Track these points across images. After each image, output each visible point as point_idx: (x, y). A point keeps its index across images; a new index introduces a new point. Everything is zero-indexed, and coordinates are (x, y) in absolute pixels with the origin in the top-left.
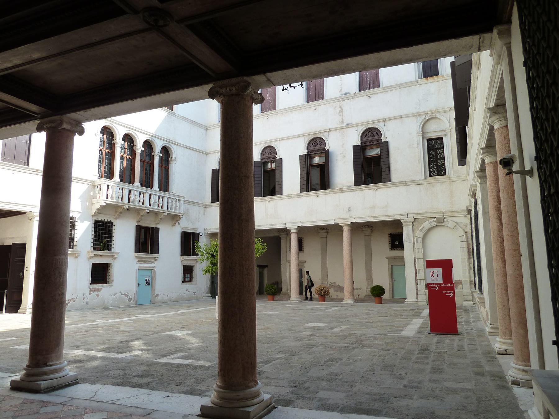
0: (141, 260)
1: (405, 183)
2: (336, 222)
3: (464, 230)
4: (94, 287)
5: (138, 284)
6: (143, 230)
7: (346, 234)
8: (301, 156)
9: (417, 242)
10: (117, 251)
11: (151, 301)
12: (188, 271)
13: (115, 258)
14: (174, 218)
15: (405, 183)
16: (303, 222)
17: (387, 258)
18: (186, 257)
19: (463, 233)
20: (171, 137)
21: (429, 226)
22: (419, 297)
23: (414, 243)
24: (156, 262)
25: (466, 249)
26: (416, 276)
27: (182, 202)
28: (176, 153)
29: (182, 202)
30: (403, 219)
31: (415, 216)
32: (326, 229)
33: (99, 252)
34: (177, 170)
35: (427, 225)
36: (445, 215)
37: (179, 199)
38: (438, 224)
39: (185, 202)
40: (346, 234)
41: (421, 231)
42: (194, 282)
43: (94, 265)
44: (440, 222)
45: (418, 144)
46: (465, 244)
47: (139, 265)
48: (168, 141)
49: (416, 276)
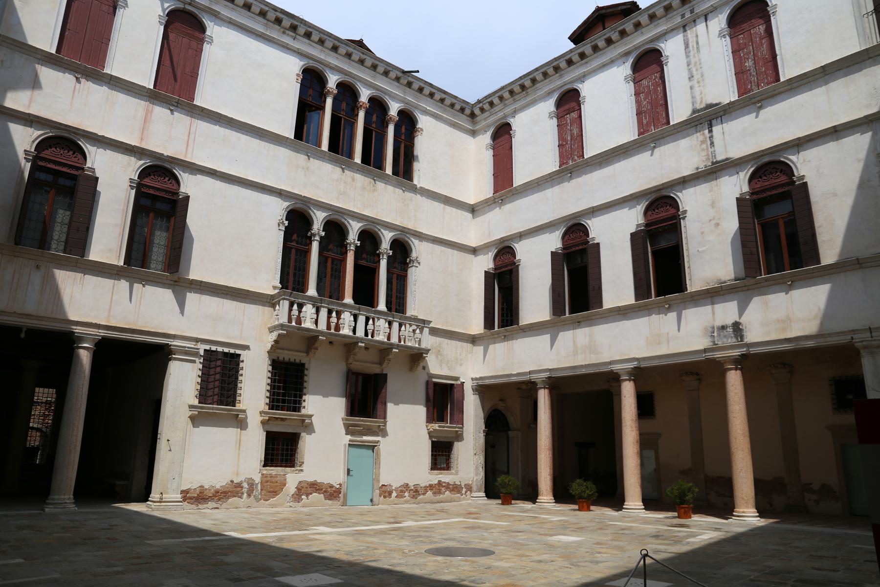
2: (709, 355)
4: (271, 472)
5: (349, 471)
6: (360, 378)
8: (632, 234)
10: (310, 413)
11: (371, 500)
14: (416, 357)
16: (644, 359)
18: (436, 426)
20: (410, 225)
27: (426, 330)
28: (419, 249)
29: (426, 330)
32: (697, 374)
33: (279, 413)
34: (419, 279)
37: (422, 323)
39: (435, 332)
47: (349, 437)
48: (404, 230)
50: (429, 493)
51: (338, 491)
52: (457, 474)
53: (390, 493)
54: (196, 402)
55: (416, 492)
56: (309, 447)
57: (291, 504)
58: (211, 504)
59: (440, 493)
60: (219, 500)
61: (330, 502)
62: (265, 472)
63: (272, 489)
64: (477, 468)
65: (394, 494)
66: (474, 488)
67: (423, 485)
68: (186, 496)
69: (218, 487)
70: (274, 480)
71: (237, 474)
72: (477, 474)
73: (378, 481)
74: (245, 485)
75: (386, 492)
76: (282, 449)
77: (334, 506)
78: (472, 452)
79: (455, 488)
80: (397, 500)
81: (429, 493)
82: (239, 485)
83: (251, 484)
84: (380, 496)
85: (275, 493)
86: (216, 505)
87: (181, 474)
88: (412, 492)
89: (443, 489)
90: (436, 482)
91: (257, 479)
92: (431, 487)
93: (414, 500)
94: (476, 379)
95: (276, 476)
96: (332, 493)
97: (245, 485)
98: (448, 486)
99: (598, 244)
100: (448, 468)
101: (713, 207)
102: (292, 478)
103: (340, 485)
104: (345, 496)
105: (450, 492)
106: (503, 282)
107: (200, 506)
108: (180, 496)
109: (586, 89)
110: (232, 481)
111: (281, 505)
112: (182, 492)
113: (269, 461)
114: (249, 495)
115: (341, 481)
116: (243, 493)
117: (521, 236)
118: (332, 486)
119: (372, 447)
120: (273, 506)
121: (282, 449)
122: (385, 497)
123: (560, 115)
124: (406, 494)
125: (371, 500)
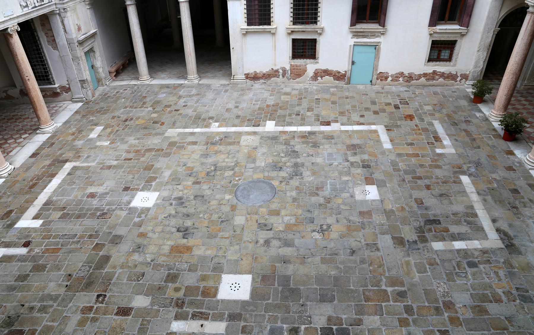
0: (356, 34)
5: (353, 63)
10: (322, 26)
11: (371, 81)
12: (441, 49)
13: (320, 34)
24: (382, 37)
43: (294, 41)
47: (356, 40)
50: (423, 79)
51: (344, 76)
52: (454, 65)
53: (386, 78)
54: (245, 26)
55: (410, 78)
56: (323, 47)
57: (311, 82)
58: (262, 81)
59: (433, 79)
60: (266, 78)
61: (337, 82)
62: (293, 63)
63: (297, 73)
64: (477, 62)
65: (390, 79)
66: (470, 78)
67: (417, 73)
68: (247, 76)
69: (264, 72)
70: (300, 68)
71: (275, 65)
72: (476, 67)
73: (377, 70)
74: (281, 71)
75: (383, 77)
76: (304, 49)
77: (341, 83)
78: (476, 49)
79: (452, 77)
80: (391, 83)
81: (423, 79)
82: (277, 71)
83: (285, 71)
84: (377, 79)
85: (299, 75)
86: (264, 82)
87: (243, 65)
88: (406, 78)
89: (437, 77)
90: (431, 71)
91: (288, 67)
92: (425, 75)
93: (407, 84)
95: (300, 66)
96: (339, 77)
97: (281, 71)
98: (442, 75)
100: (450, 59)
102: (311, 67)
103: (346, 72)
104: (349, 79)
105: (444, 79)
107: (256, 82)
108: (244, 76)
110: (272, 69)
111: (304, 82)
112: (245, 74)
113: (295, 56)
114: (283, 76)
115: (346, 69)
116: (279, 75)
118: (339, 72)
119: (376, 47)
120: (298, 83)
121: (304, 49)
122: (381, 80)
124: (401, 79)
125: (371, 81)
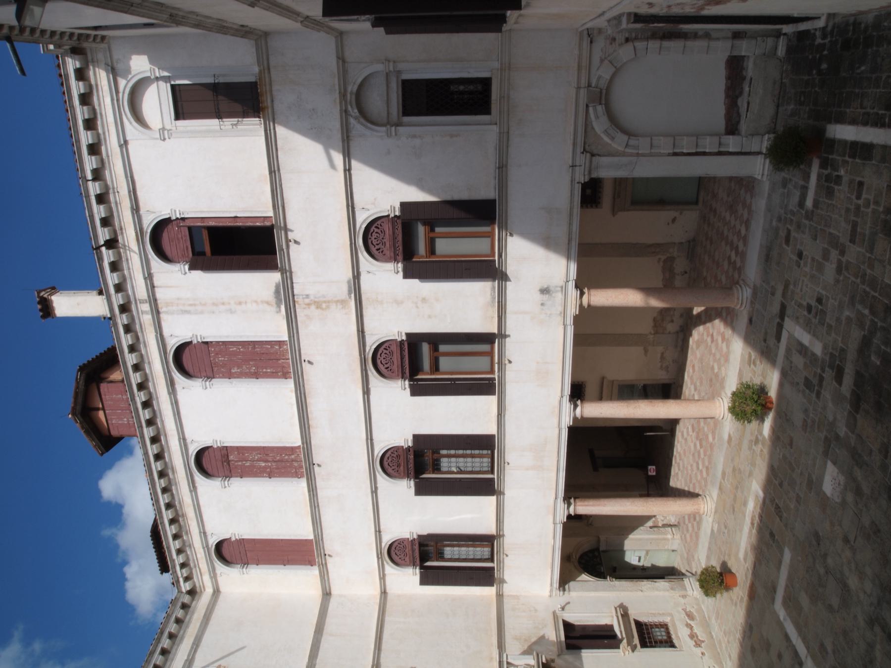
1: (502, 169)
2: (570, 321)
3: (621, 45)
7: (602, 298)
9: (637, 147)
15: (502, 169)
17: (614, 213)
19: (630, 46)
21: (604, 119)
22: (755, 149)
23: (638, 155)
25: (666, 43)
26: (710, 154)
30: (581, 177)
31: (579, 149)
35: (600, 125)
36: (584, 82)
38: (603, 102)
40: (602, 298)
41: (613, 138)
42: (667, 620)
44: (601, 96)
45: (414, 136)
46: (654, 45)
49: (710, 154)
94: (551, 591)
99: (416, 437)
101: (402, 302)
106: (429, 557)
109: (199, 438)
117: (378, 532)
123: (227, 473)
